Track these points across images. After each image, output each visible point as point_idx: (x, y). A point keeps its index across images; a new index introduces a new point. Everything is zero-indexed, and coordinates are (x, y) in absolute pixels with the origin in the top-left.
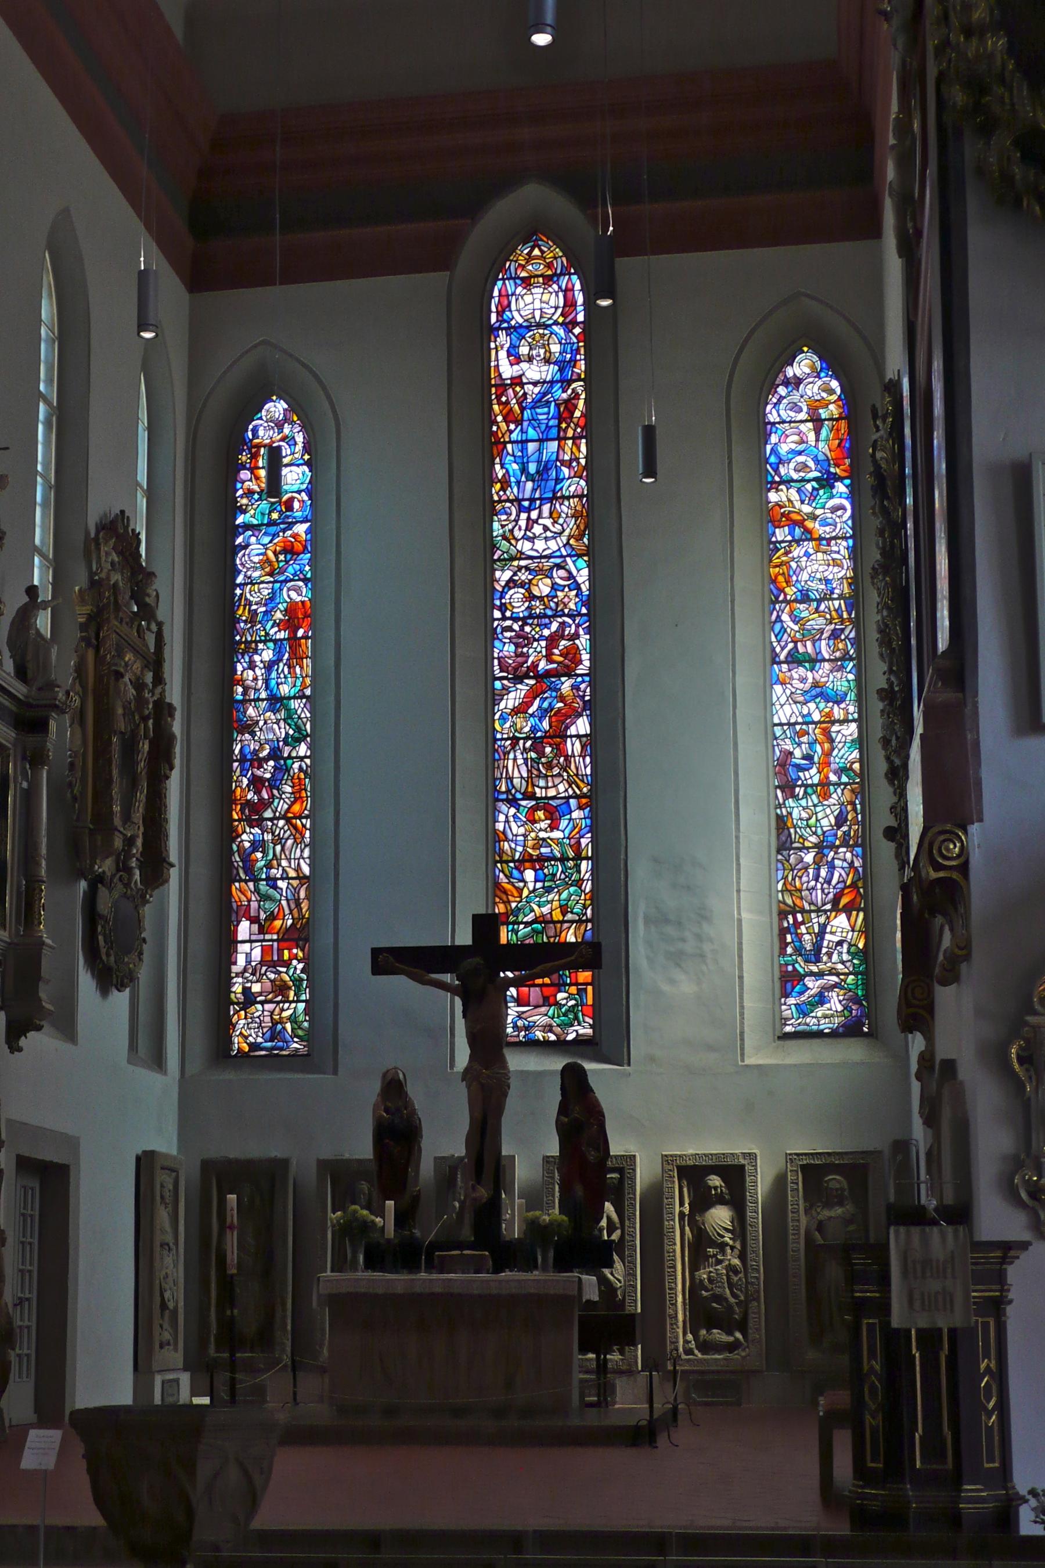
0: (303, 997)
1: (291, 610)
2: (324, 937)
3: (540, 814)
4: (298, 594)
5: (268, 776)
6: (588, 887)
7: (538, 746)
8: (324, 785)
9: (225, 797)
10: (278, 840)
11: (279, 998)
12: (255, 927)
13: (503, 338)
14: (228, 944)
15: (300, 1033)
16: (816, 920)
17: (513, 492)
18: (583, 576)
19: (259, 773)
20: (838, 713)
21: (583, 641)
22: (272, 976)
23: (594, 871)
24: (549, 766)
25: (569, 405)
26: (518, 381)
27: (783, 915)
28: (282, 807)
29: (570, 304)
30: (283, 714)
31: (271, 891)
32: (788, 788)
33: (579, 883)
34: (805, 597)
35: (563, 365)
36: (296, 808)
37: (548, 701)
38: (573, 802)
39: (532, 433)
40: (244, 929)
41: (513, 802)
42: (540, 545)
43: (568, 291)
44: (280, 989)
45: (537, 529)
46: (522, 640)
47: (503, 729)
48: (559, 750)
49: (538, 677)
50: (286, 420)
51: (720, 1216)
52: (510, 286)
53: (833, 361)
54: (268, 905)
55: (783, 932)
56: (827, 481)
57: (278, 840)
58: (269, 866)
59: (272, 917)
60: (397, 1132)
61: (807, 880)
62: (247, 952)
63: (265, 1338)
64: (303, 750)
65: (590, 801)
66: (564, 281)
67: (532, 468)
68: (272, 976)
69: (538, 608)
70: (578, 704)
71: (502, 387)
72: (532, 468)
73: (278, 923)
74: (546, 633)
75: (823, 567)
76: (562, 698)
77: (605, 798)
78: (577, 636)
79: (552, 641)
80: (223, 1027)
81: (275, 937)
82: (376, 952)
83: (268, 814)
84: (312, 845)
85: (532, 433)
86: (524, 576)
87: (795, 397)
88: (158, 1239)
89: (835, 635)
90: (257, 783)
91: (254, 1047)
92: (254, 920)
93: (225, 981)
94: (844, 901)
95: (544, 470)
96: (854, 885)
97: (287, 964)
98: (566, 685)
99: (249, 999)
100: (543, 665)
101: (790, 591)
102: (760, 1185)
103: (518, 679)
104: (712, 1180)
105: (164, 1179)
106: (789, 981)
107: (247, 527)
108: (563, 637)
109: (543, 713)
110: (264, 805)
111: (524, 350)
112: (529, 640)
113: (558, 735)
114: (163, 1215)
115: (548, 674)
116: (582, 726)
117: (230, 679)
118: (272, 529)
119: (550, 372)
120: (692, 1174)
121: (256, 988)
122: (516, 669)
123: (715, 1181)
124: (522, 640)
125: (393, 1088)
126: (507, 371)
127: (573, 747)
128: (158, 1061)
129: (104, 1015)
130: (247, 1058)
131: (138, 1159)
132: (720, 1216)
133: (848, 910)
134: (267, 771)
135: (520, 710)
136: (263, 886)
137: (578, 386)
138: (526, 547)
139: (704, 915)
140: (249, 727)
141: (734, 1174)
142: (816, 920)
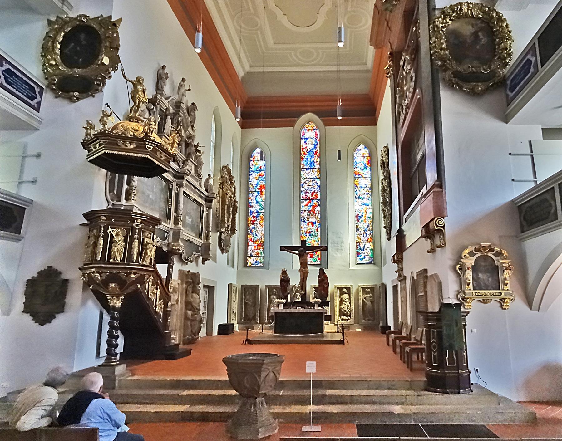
2: (266, 245)
3: (310, 224)
4: (263, 183)
6: (319, 237)
7: (310, 211)
9: (247, 219)
13: (303, 140)
14: (247, 246)
16: (364, 244)
17: (305, 167)
18: (319, 182)
20: (368, 207)
21: (319, 194)
23: (321, 234)
25: (316, 152)
26: (306, 147)
27: (357, 243)
28: (258, 221)
29: (316, 135)
32: (358, 220)
34: (361, 187)
35: (315, 145)
36: (261, 222)
39: (309, 157)
40: (251, 243)
41: (305, 222)
42: (310, 177)
44: (258, 254)
45: (310, 174)
46: (307, 193)
47: (303, 209)
48: (314, 213)
49: (310, 200)
51: (345, 296)
54: (256, 239)
55: (357, 246)
59: (256, 241)
60: (285, 281)
61: (362, 236)
62: (251, 247)
63: (254, 318)
64: (263, 211)
65: (320, 222)
67: (309, 163)
69: (310, 187)
71: (303, 149)
72: (309, 163)
75: (365, 182)
77: (323, 221)
79: (313, 193)
80: (246, 261)
84: (265, 228)
85: (309, 157)
86: (307, 182)
87: (360, 152)
88: (233, 300)
89: (367, 194)
91: (252, 264)
93: (246, 252)
95: (311, 164)
98: (315, 201)
99: (251, 256)
100: (311, 198)
101: (359, 186)
102: (353, 291)
103: (306, 200)
104: (344, 290)
105: (234, 289)
106: (358, 254)
109: (311, 206)
110: (255, 221)
111: (307, 142)
112: (308, 193)
114: (233, 295)
116: (318, 208)
117: (248, 198)
119: (313, 146)
120: (340, 289)
121: (253, 254)
124: (307, 193)
125: (284, 272)
126: (304, 145)
128: (233, 267)
129: (222, 258)
130: (251, 266)
132: (345, 296)
135: (307, 205)
136: (254, 235)
137: (318, 149)
138: (308, 177)
139: (342, 242)
141: (348, 289)
142: (364, 244)
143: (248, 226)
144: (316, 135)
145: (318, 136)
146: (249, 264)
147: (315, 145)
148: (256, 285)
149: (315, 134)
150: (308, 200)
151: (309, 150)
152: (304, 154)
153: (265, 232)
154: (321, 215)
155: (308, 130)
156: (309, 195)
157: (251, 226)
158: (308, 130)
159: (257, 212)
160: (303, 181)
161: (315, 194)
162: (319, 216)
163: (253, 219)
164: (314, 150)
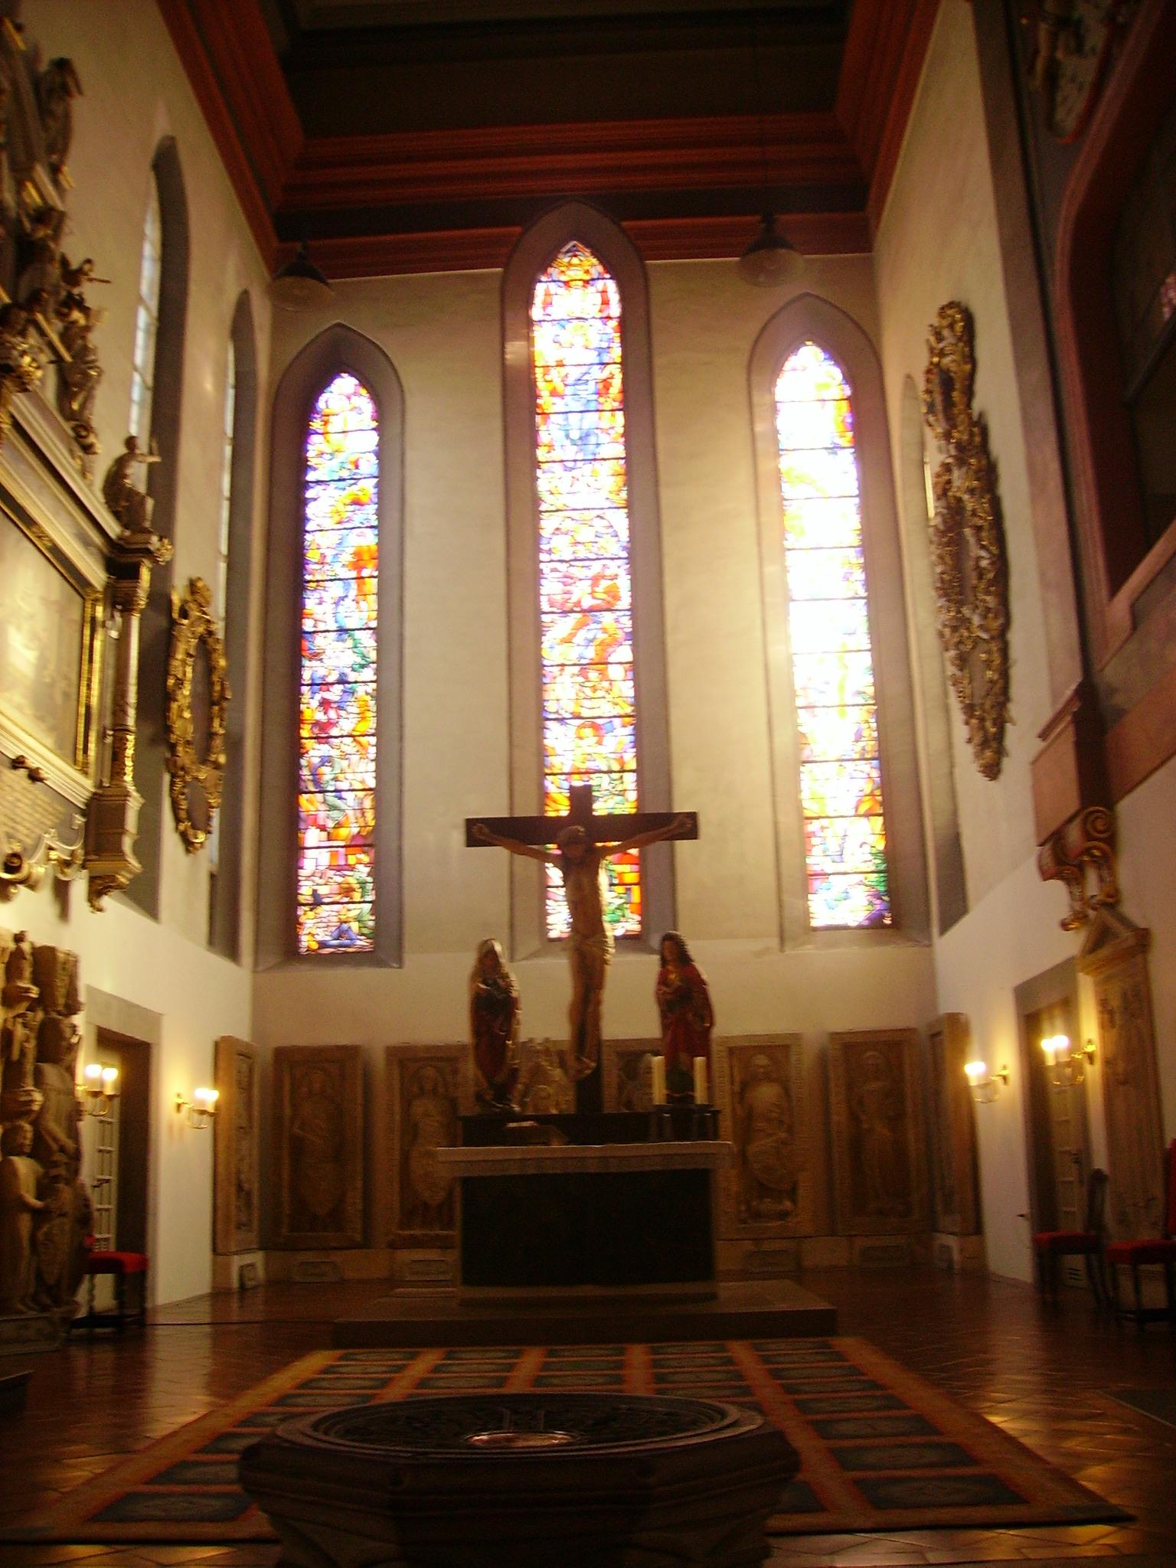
0: (369, 898)
1: (358, 555)
3: (588, 732)
5: (337, 698)
8: (389, 701)
10: (345, 756)
11: (346, 900)
12: (324, 834)
15: (365, 931)
17: (556, 455)
19: (327, 695)
22: (340, 879)
24: (594, 689)
25: (606, 384)
29: (605, 302)
30: (350, 643)
31: (339, 803)
33: (622, 793)
37: (591, 632)
38: (617, 722)
40: (312, 837)
41: (561, 720)
43: (604, 292)
44: (348, 891)
45: (577, 486)
46: (568, 580)
50: (355, 394)
52: (553, 287)
53: (837, 352)
54: (335, 814)
56: (835, 448)
57: (345, 756)
58: (336, 779)
59: (339, 825)
62: (314, 860)
66: (600, 284)
68: (340, 879)
70: (620, 635)
72: (575, 435)
73: (343, 832)
74: (591, 573)
76: (604, 630)
78: (615, 577)
79: (595, 580)
80: (291, 926)
81: (342, 843)
82: (470, 823)
83: (334, 732)
86: (568, 525)
90: (325, 704)
91: (323, 945)
92: (323, 828)
94: (863, 809)
95: (585, 437)
96: (872, 794)
97: (352, 868)
98: (607, 618)
99: (317, 902)
100: (587, 602)
103: (565, 613)
107: (318, 482)
108: (604, 577)
110: (331, 723)
113: (602, 663)
115: (591, 610)
118: (341, 484)
121: (323, 890)
122: (563, 605)
123: (761, 1060)
124: (568, 580)
127: (616, 672)
131: (217, 1045)
133: (868, 815)
134: (335, 693)
136: (330, 797)
140: (316, 656)
143: (296, 750)
144: (605, 302)
145: (615, 310)
146: (307, 942)
147: (601, 351)
148: (344, 1048)
149: (598, 299)
150: (574, 618)
151: (574, 374)
152: (554, 393)
153: (378, 778)
154: (636, 687)
155: (567, 284)
156: (581, 593)
157: (314, 752)
158: (567, 284)
159: (342, 681)
160: (547, 524)
161: (604, 584)
162: (627, 689)
163: (321, 716)
164: (598, 374)
